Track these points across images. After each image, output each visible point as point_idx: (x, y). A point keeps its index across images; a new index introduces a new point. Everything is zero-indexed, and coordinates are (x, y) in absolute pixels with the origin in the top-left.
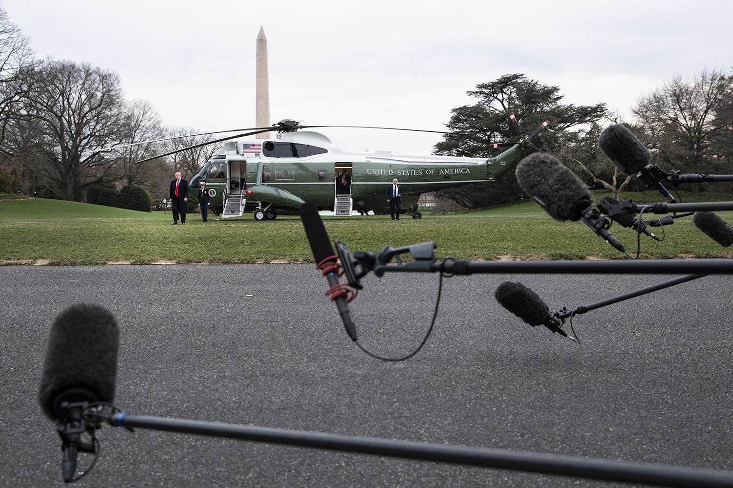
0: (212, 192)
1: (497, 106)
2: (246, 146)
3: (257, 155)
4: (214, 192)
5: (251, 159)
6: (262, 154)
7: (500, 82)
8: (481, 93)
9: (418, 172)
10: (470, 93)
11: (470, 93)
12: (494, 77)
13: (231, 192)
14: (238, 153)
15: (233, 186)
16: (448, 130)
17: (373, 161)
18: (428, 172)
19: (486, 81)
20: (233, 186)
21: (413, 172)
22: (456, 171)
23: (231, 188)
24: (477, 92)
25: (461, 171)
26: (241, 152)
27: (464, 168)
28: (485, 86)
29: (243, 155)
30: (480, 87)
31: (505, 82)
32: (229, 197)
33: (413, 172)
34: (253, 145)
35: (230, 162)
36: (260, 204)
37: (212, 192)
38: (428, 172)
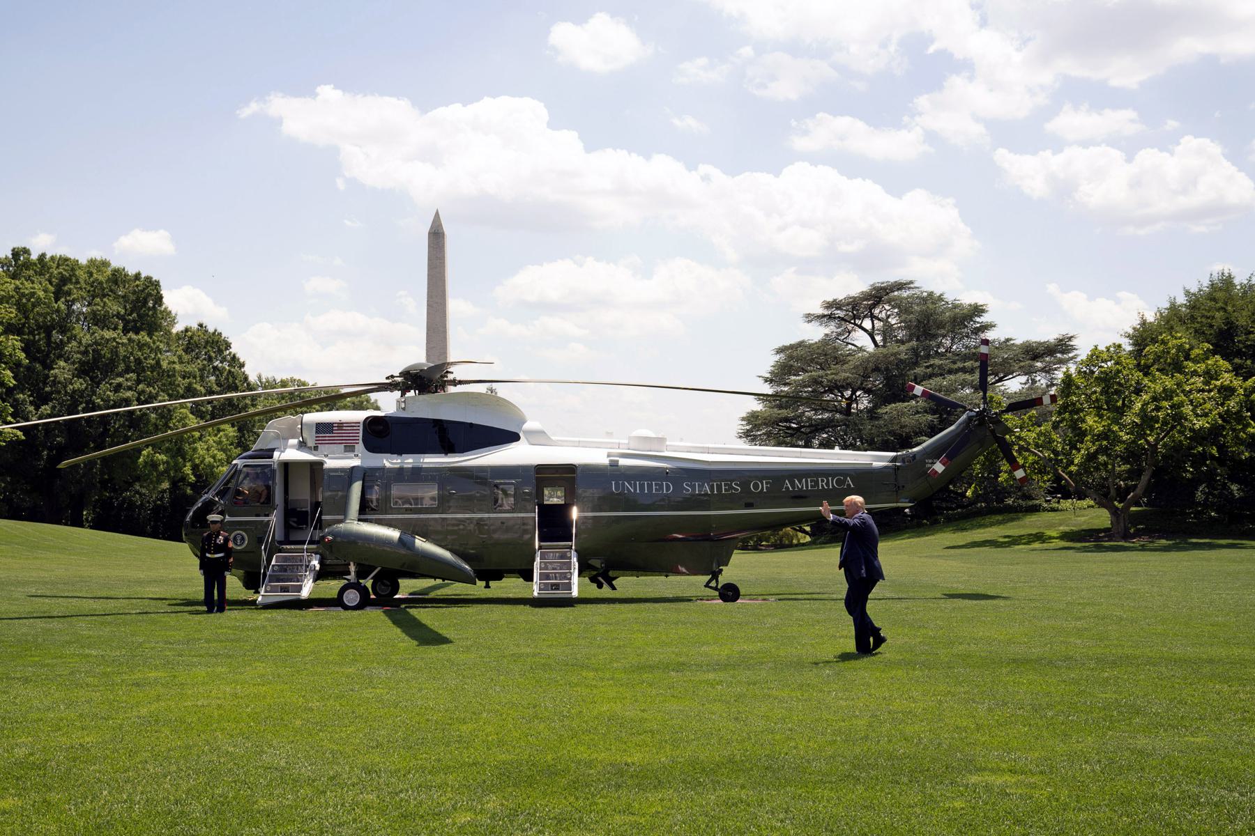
0: (239, 538)
2: (323, 428)
3: (350, 448)
4: (243, 539)
6: (360, 447)
7: (866, 296)
10: (810, 318)
11: (810, 318)
12: (854, 285)
13: (287, 535)
16: (768, 389)
17: (623, 462)
18: (756, 486)
19: (841, 296)
21: (719, 487)
22: (822, 484)
23: (288, 527)
24: (824, 316)
28: (835, 304)
29: (316, 448)
30: (829, 305)
31: (878, 295)
33: (719, 487)
35: (286, 465)
36: (352, 568)
37: (239, 538)
38: (756, 486)
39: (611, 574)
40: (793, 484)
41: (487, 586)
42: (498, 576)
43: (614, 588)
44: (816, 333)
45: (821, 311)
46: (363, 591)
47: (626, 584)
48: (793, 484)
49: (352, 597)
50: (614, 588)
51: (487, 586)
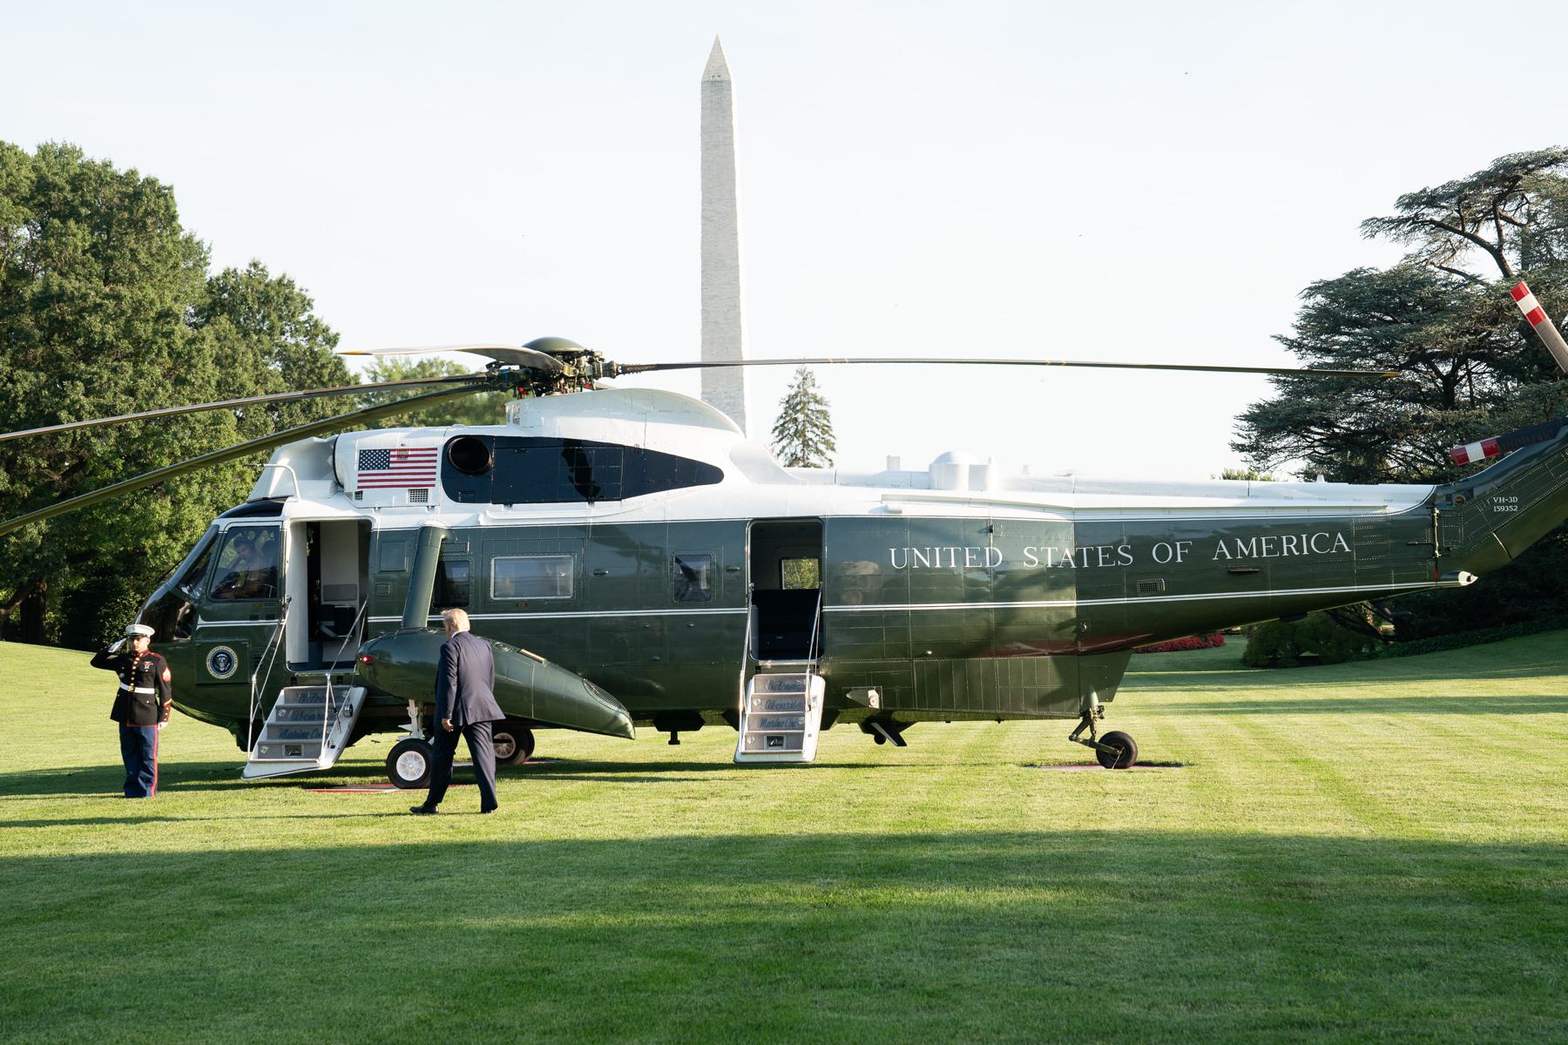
2: (373, 460)
3: (420, 494)
4: (229, 660)
6: (437, 492)
7: (1485, 179)
8: (1417, 222)
9: (1114, 555)
10: (1375, 225)
14: (339, 485)
15: (326, 628)
18: (1162, 553)
20: (326, 628)
21: (1093, 555)
22: (1288, 547)
25: (1310, 545)
26: (351, 486)
27: (1327, 528)
28: (1432, 200)
29: (359, 495)
30: (1411, 201)
31: (1507, 179)
32: (294, 681)
33: (1093, 555)
34: (403, 455)
38: (1162, 553)
39: (898, 716)
40: (1233, 549)
41: (674, 741)
43: (901, 743)
44: (1385, 256)
45: (1397, 213)
48: (1233, 549)
50: (901, 743)
51: (674, 741)
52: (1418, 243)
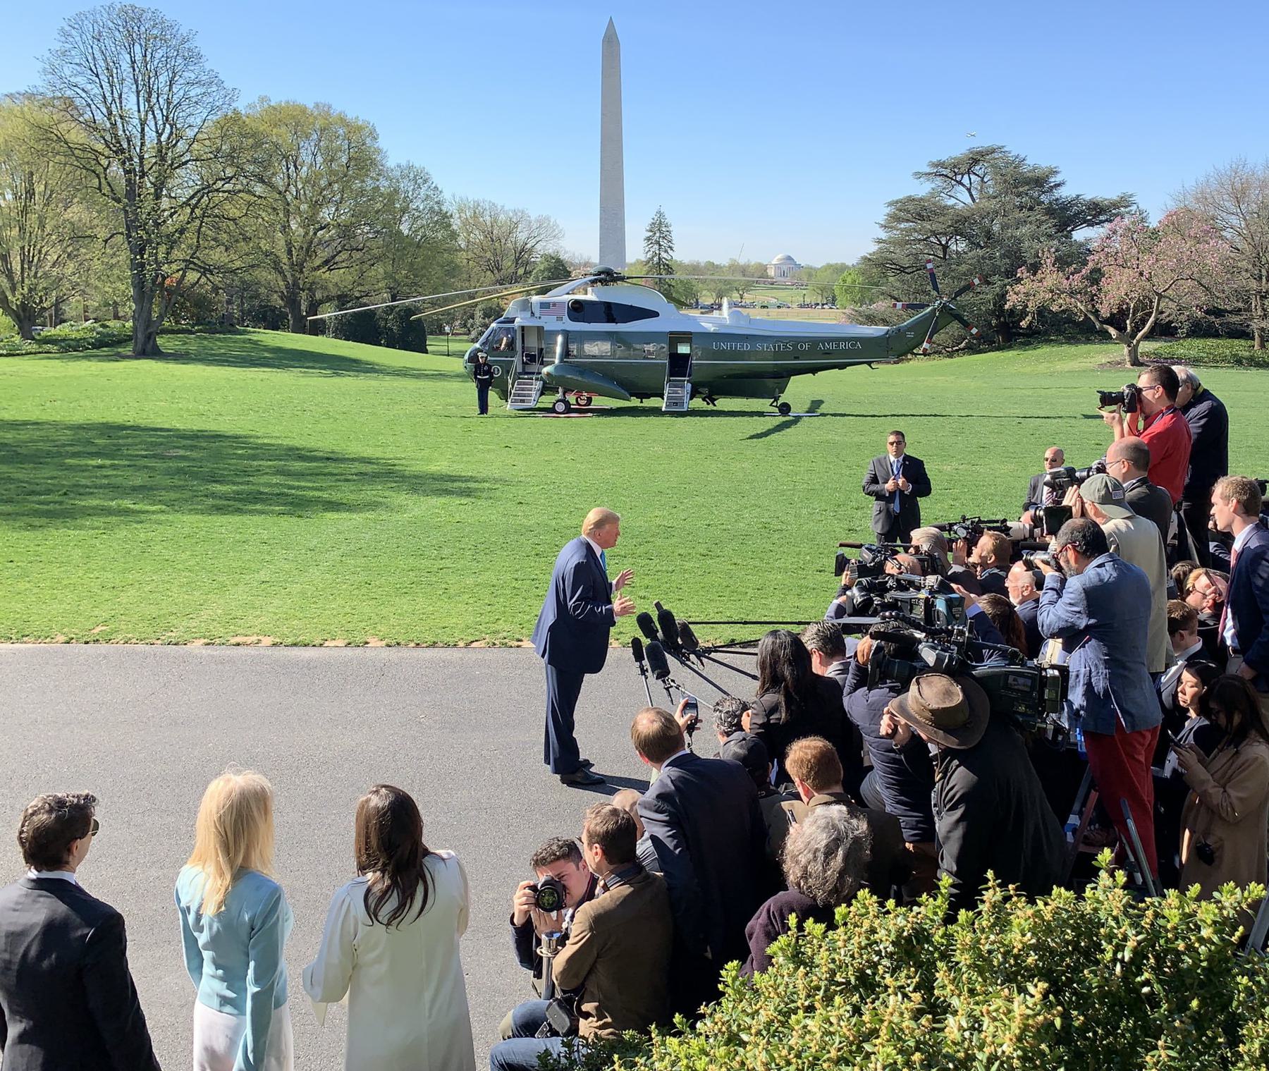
1: (960, 199)
2: (544, 305)
5: (550, 323)
6: (566, 318)
10: (918, 175)
11: (918, 175)
12: (957, 149)
16: (883, 235)
22: (842, 346)
28: (941, 164)
30: (936, 165)
31: (975, 159)
34: (554, 304)
42: (648, 396)
44: (922, 189)
45: (928, 170)
46: (567, 403)
47: (723, 403)
49: (561, 407)
52: (939, 181)
